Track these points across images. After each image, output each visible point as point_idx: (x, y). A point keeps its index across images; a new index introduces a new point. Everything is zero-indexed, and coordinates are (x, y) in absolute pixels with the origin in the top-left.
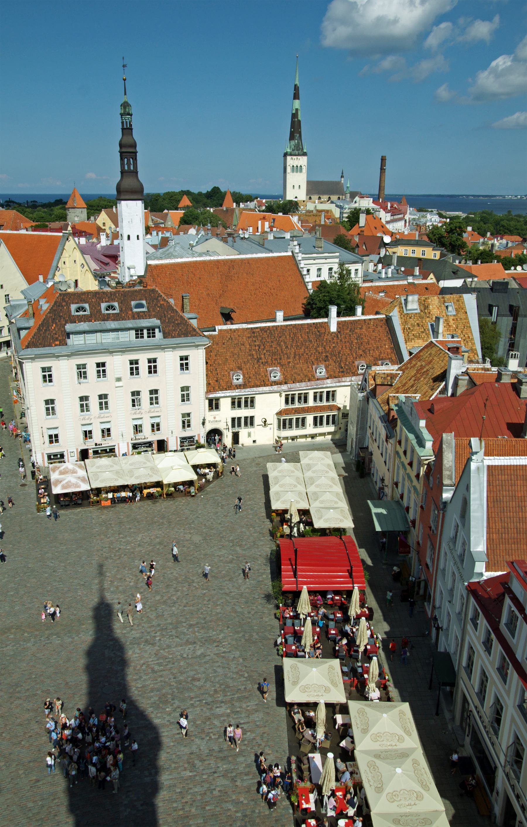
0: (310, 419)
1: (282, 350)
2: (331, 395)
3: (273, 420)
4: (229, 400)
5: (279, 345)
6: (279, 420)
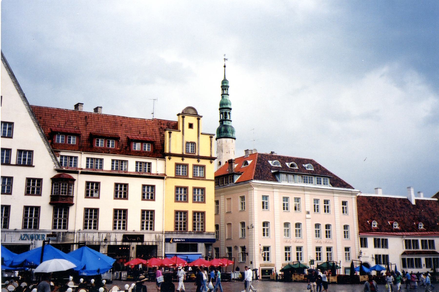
0: (423, 261)
2: (432, 243)
6: (403, 260)
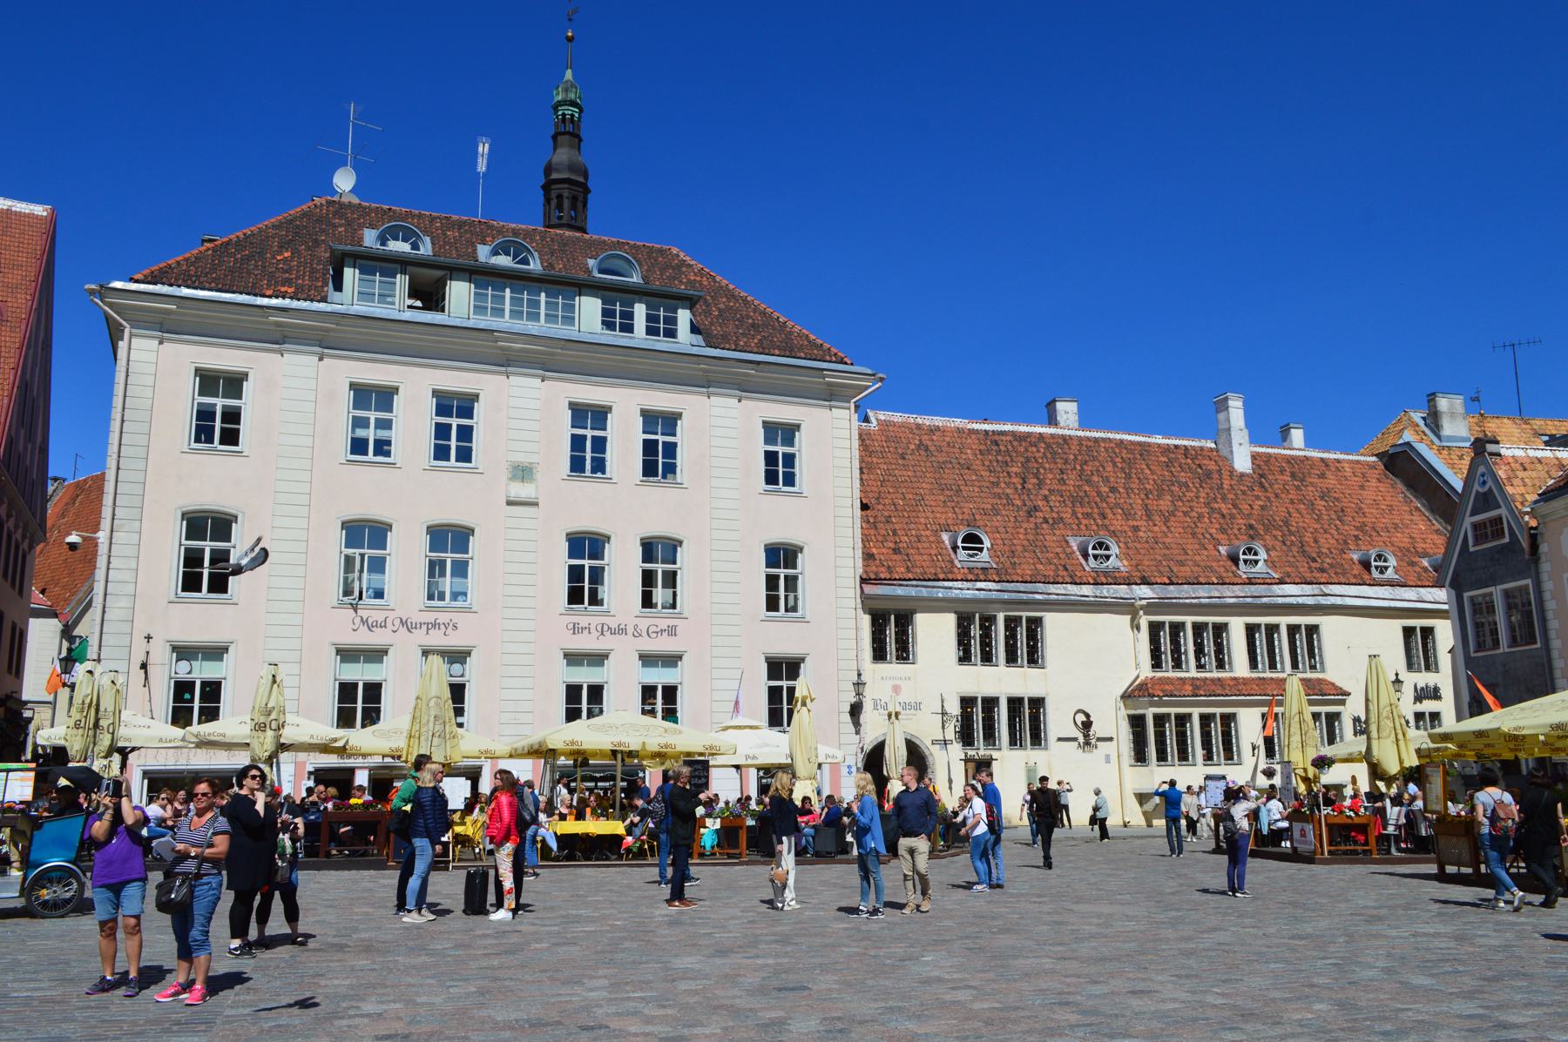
1: (1099, 493)
3: (1112, 722)
4: (949, 621)
5: (1088, 482)
6: (1137, 722)
